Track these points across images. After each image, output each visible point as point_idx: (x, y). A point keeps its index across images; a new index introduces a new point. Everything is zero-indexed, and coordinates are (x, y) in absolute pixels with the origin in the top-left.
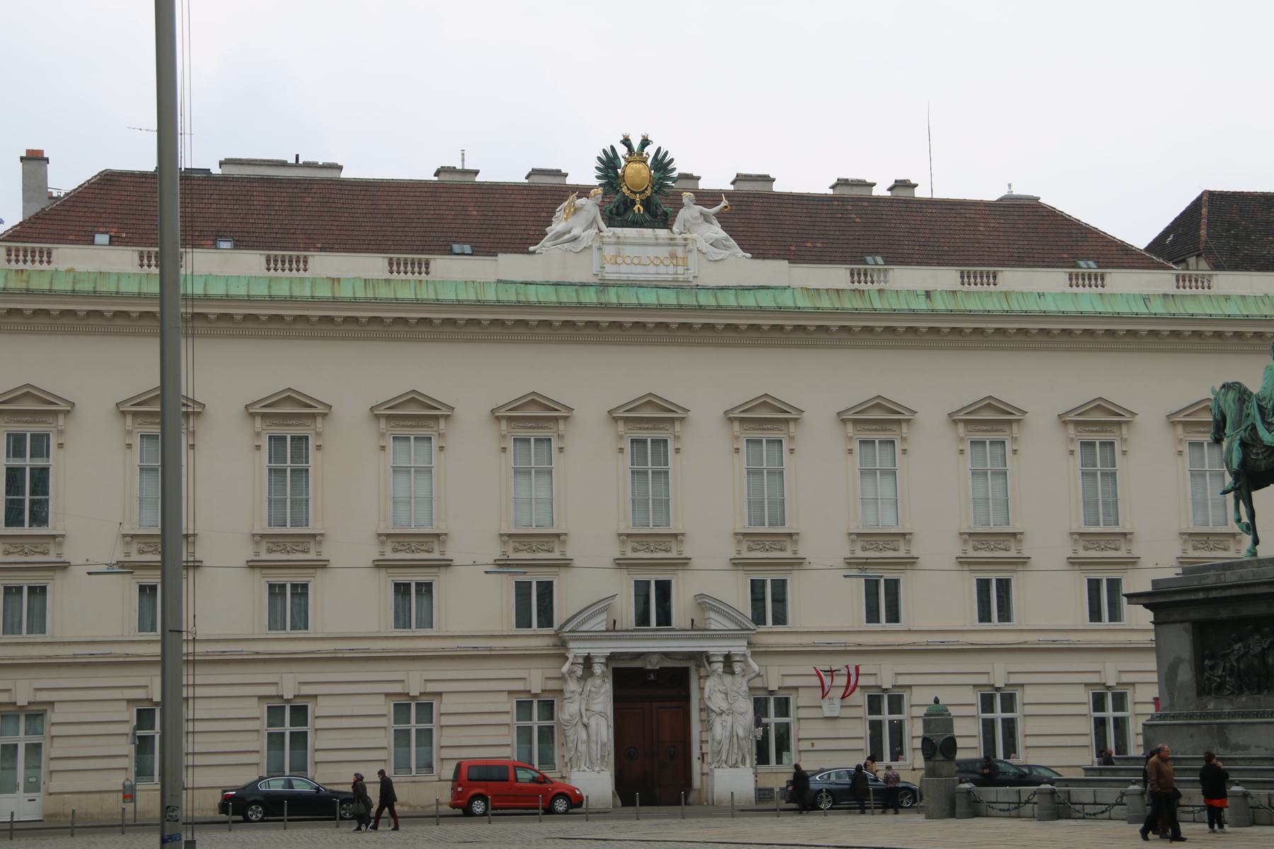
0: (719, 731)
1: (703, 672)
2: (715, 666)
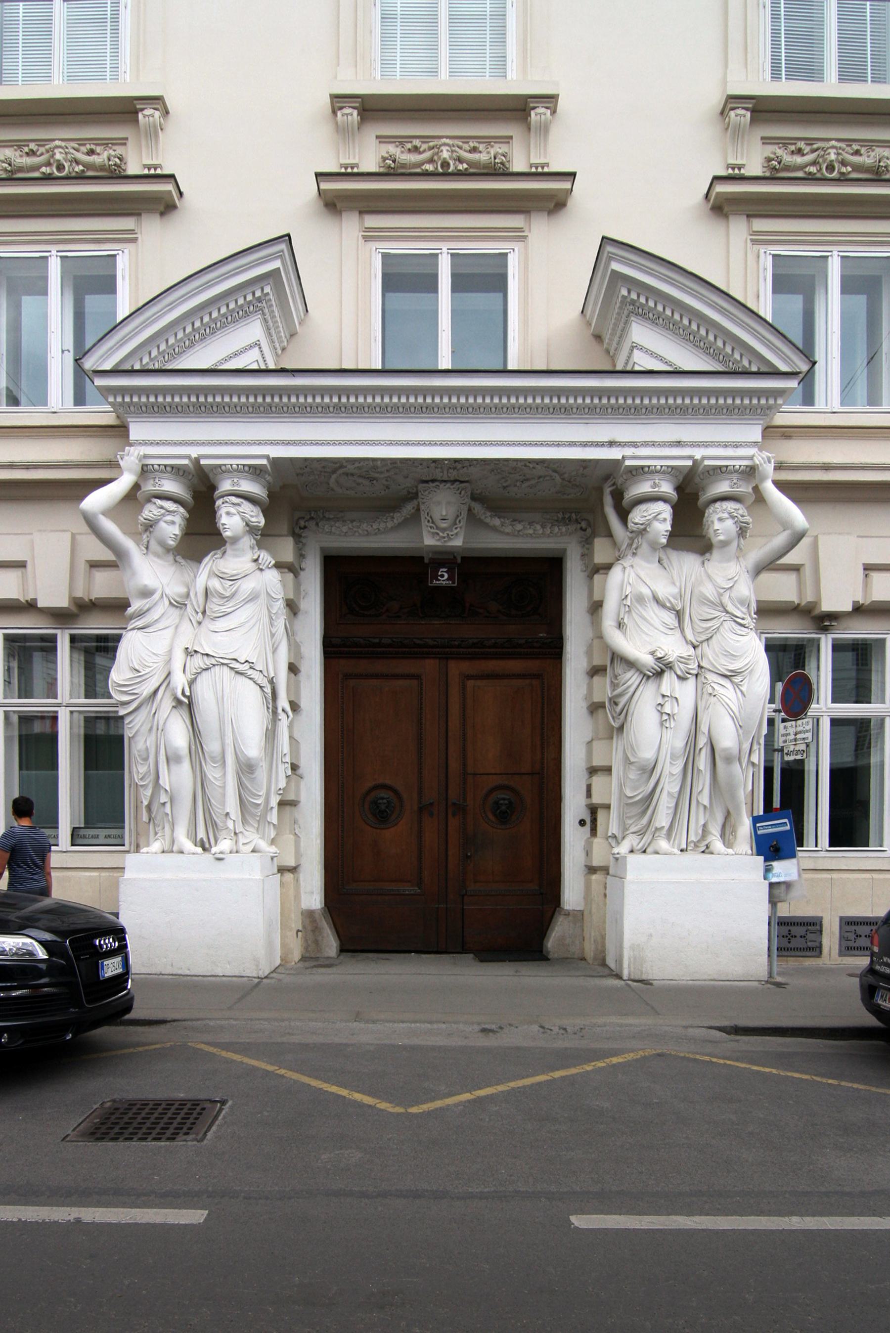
0: (653, 729)
1: (601, 552)
2: (637, 516)
